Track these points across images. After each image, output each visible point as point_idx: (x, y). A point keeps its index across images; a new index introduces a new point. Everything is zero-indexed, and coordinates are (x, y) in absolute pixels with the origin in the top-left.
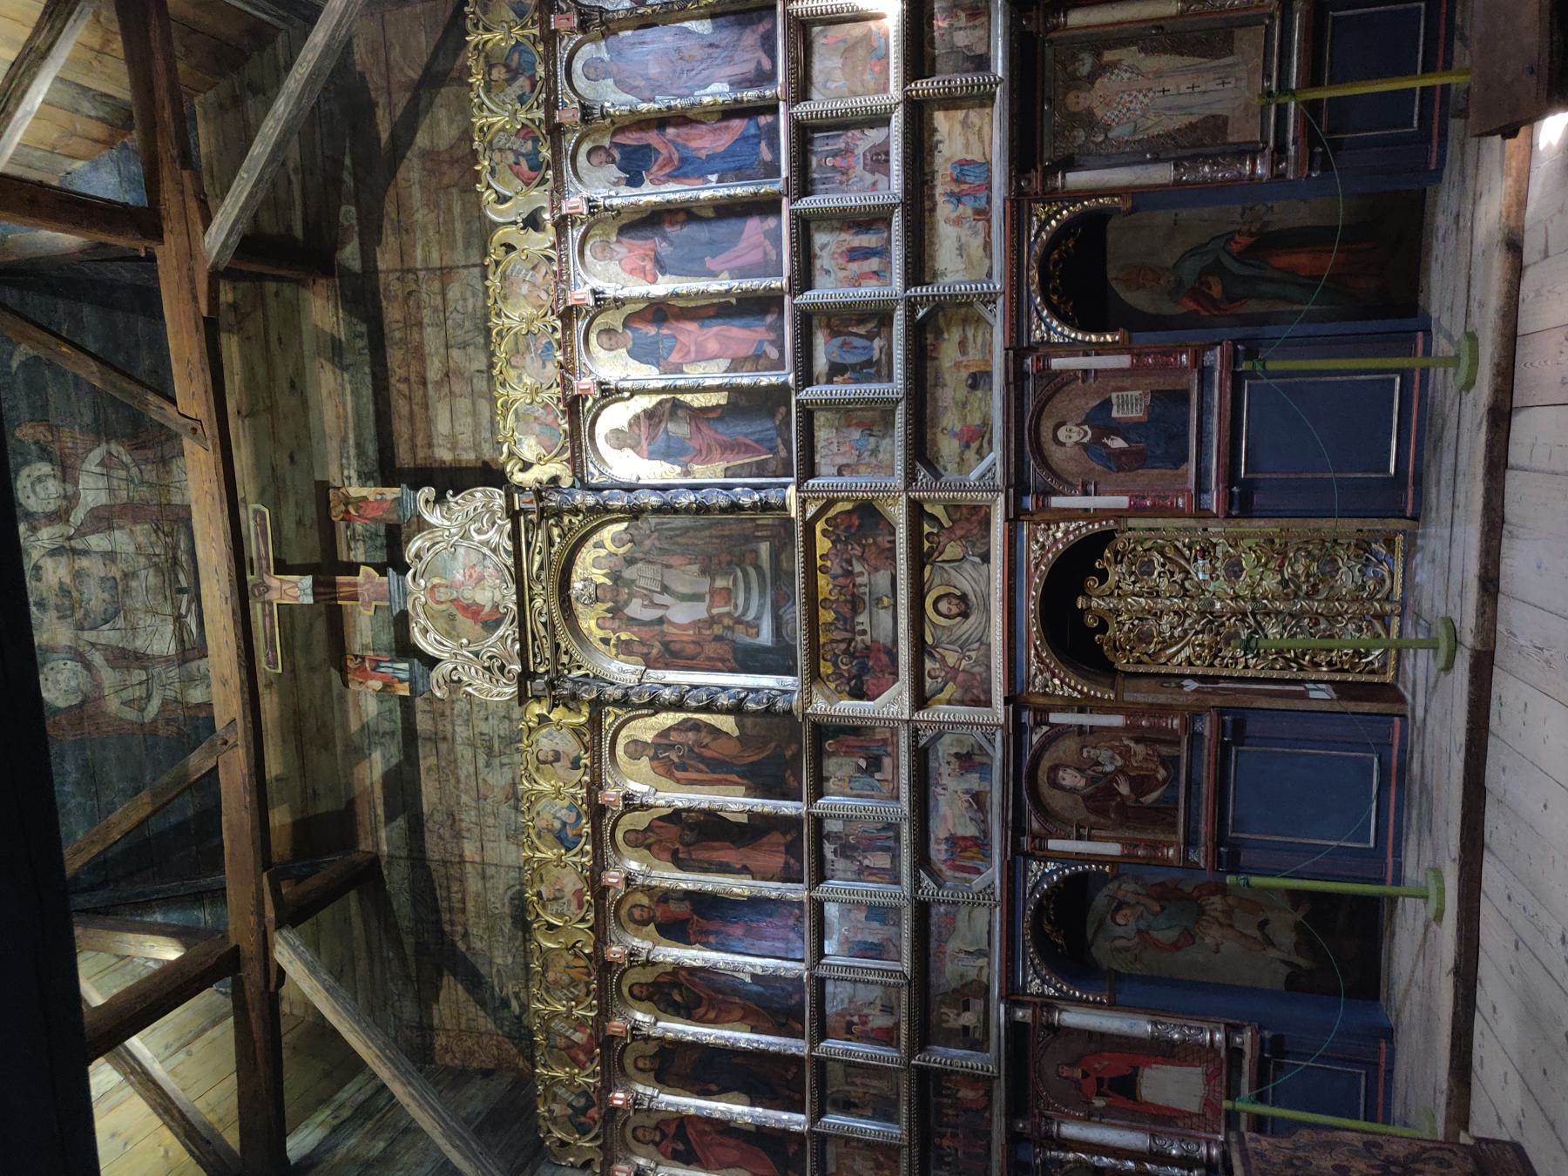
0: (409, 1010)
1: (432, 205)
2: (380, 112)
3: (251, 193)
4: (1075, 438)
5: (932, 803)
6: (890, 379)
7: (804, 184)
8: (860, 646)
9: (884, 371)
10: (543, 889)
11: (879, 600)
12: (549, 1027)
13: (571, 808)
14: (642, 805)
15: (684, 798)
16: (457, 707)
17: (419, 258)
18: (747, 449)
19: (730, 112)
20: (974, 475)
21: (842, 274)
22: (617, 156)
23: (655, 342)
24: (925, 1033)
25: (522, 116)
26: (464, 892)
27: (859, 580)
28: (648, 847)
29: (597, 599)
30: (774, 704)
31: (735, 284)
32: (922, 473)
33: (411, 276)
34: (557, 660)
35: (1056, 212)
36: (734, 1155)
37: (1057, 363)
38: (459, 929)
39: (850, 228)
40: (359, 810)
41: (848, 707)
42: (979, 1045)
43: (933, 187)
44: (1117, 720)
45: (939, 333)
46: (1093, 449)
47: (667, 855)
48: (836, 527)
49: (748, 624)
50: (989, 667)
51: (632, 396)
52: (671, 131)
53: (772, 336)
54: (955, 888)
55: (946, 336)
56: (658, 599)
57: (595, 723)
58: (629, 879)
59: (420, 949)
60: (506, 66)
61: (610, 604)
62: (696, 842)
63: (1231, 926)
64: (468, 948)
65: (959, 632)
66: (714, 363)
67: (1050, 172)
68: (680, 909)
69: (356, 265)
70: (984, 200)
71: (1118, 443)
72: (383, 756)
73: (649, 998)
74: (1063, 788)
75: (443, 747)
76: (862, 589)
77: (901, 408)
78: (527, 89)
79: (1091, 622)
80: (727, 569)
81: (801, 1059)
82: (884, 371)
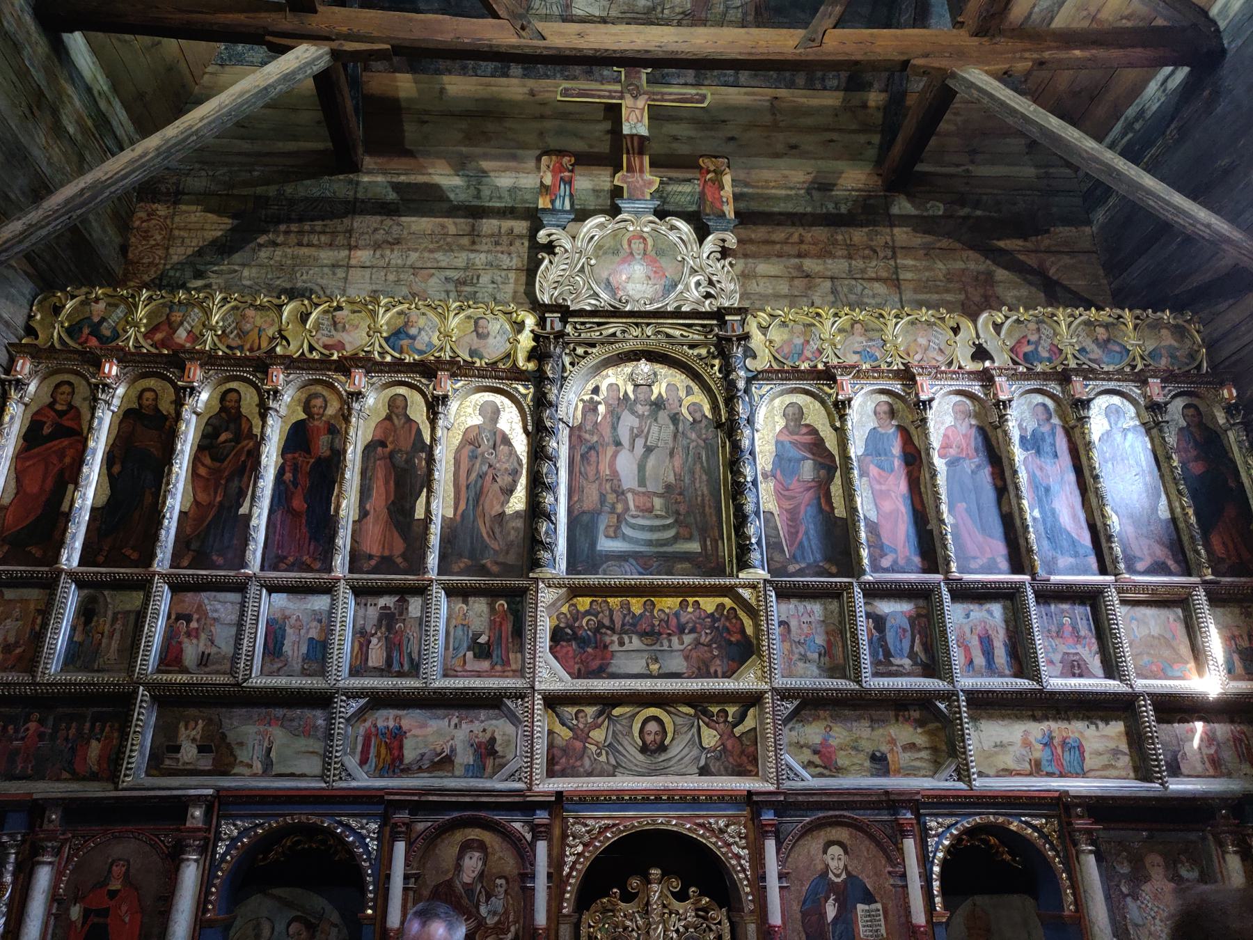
0: (197, 183)
1: (949, 277)
2: (1020, 242)
3: (1016, 111)
4: (833, 865)
5: (440, 712)
6: (876, 674)
7: (1049, 595)
8: (607, 639)
10: (345, 312)
11: (656, 660)
12: (193, 305)
13: (430, 344)
14: (436, 414)
15: (444, 455)
16: (505, 257)
17: (905, 262)
18: (793, 534)
21: (968, 631)
22: (1045, 429)
24: (173, 702)
25: (1069, 350)
26: (319, 247)
27: (675, 640)
28: (388, 418)
29: (636, 386)
30: (545, 549)
32: (791, 706)
33: (890, 254)
34: (579, 344)
35: (1051, 843)
36: (32, 488)
37: (910, 845)
38: (280, 239)
39: (1010, 638)
40: (404, 160)
41: (545, 625)
42: (156, 764)
43: (1055, 719)
44: (541, 919)
45: (921, 723)
46: (823, 884)
48: (727, 618)
49: (618, 528)
50: (590, 774)
51: (836, 429)
53: (901, 562)
54: (346, 736)
55: (919, 730)
56: (640, 443)
57: (517, 374)
58: (358, 395)
59: (262, 201)
60: (1108, 340)
61: (632, 396)
62: (394, 465)
64: (260, 246)
65: (625, 743)
66: (872, 506)
68: (322, 444)
69: (895, 210)
70: (1049, 769)
71: (831, 911)
72: (456, 187)
73: (223, 409)
74: (460, 857)
75: (465, 241)
76: (666, 643)
77: (853, 686)
78: (1092, 356)
79: (635, 882)
81: (150, 565)
82: (882, 669)
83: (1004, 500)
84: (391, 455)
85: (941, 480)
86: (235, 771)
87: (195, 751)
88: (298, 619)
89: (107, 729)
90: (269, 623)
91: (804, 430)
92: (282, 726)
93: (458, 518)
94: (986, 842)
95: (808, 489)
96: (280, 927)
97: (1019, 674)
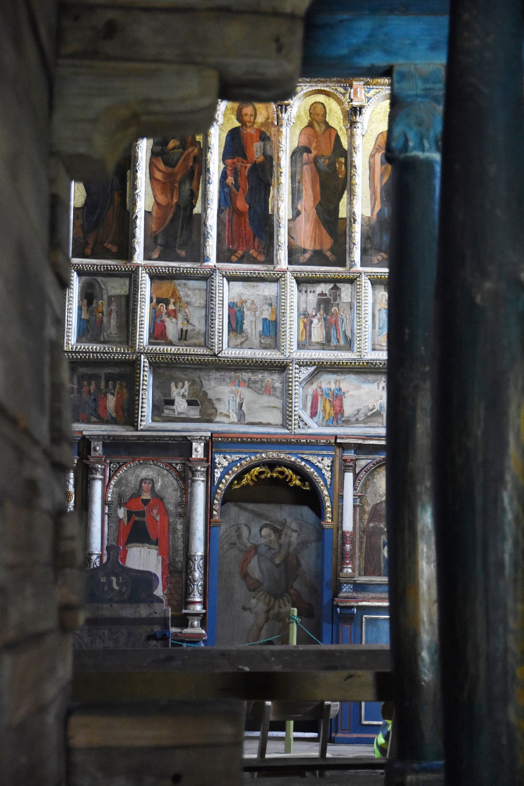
5: (371, 377)
28: (310, 125)
47: (304, 142)
63: (267, 619)
68: (256, 151)
84: (315, 161)
86: (218, 419)
87: (186, 404)
88: (253, 303)
89: (118, 386)
90: (231, 307)
92: (249, 387)
93: (375, 217)
96: (255, 530)
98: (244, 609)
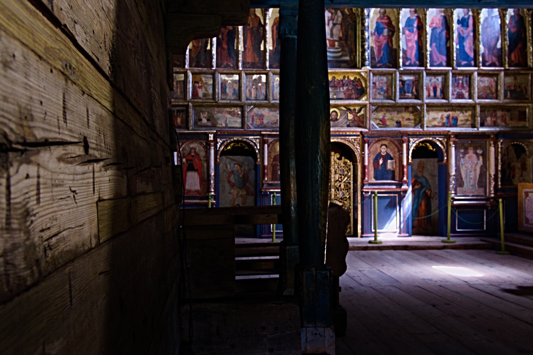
4: (383, 150)
6: (400, 98)
9: (402, 97)
11: (335, 95)
19: (476, 52)
20: (372, 122)
21: (430, 84)
22: (466, 17)
23: (412, 26)
27: (341, 89)
31: (428, 53)
37: (405, 145)
46: (379, 156)
48: (357, 82)
52: (472, 34)
53: (412, 63)
56: (331, 22)
63: (237, 197)
66: (405, 45)
67: (455, 143)
71: (381, 162)
80: (341, 46)
83: (448, 43)
85: (429, 36)
90: (222, 84)
91: (386, 18)
94: (426, 145)
95: (385, 39)
96: (232, 165)
97: (444, 98)
98: (229, 193)
